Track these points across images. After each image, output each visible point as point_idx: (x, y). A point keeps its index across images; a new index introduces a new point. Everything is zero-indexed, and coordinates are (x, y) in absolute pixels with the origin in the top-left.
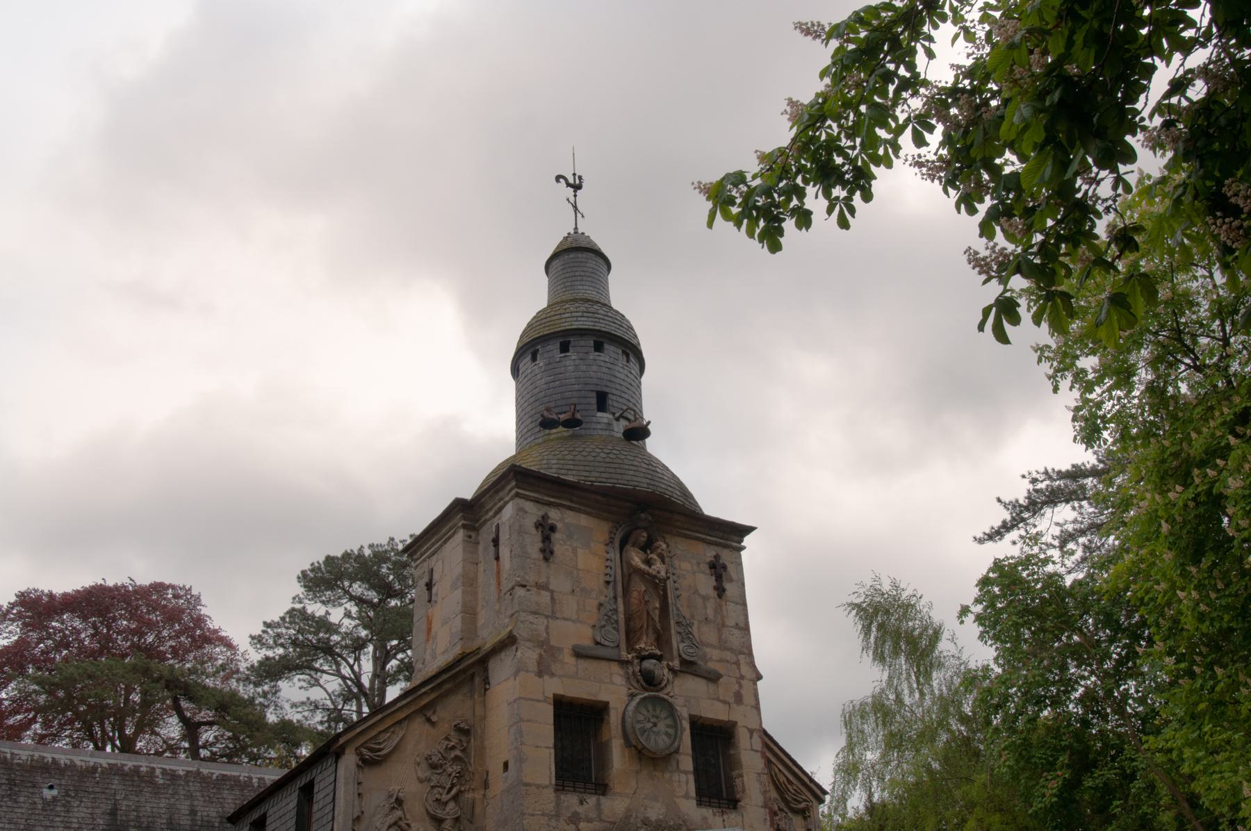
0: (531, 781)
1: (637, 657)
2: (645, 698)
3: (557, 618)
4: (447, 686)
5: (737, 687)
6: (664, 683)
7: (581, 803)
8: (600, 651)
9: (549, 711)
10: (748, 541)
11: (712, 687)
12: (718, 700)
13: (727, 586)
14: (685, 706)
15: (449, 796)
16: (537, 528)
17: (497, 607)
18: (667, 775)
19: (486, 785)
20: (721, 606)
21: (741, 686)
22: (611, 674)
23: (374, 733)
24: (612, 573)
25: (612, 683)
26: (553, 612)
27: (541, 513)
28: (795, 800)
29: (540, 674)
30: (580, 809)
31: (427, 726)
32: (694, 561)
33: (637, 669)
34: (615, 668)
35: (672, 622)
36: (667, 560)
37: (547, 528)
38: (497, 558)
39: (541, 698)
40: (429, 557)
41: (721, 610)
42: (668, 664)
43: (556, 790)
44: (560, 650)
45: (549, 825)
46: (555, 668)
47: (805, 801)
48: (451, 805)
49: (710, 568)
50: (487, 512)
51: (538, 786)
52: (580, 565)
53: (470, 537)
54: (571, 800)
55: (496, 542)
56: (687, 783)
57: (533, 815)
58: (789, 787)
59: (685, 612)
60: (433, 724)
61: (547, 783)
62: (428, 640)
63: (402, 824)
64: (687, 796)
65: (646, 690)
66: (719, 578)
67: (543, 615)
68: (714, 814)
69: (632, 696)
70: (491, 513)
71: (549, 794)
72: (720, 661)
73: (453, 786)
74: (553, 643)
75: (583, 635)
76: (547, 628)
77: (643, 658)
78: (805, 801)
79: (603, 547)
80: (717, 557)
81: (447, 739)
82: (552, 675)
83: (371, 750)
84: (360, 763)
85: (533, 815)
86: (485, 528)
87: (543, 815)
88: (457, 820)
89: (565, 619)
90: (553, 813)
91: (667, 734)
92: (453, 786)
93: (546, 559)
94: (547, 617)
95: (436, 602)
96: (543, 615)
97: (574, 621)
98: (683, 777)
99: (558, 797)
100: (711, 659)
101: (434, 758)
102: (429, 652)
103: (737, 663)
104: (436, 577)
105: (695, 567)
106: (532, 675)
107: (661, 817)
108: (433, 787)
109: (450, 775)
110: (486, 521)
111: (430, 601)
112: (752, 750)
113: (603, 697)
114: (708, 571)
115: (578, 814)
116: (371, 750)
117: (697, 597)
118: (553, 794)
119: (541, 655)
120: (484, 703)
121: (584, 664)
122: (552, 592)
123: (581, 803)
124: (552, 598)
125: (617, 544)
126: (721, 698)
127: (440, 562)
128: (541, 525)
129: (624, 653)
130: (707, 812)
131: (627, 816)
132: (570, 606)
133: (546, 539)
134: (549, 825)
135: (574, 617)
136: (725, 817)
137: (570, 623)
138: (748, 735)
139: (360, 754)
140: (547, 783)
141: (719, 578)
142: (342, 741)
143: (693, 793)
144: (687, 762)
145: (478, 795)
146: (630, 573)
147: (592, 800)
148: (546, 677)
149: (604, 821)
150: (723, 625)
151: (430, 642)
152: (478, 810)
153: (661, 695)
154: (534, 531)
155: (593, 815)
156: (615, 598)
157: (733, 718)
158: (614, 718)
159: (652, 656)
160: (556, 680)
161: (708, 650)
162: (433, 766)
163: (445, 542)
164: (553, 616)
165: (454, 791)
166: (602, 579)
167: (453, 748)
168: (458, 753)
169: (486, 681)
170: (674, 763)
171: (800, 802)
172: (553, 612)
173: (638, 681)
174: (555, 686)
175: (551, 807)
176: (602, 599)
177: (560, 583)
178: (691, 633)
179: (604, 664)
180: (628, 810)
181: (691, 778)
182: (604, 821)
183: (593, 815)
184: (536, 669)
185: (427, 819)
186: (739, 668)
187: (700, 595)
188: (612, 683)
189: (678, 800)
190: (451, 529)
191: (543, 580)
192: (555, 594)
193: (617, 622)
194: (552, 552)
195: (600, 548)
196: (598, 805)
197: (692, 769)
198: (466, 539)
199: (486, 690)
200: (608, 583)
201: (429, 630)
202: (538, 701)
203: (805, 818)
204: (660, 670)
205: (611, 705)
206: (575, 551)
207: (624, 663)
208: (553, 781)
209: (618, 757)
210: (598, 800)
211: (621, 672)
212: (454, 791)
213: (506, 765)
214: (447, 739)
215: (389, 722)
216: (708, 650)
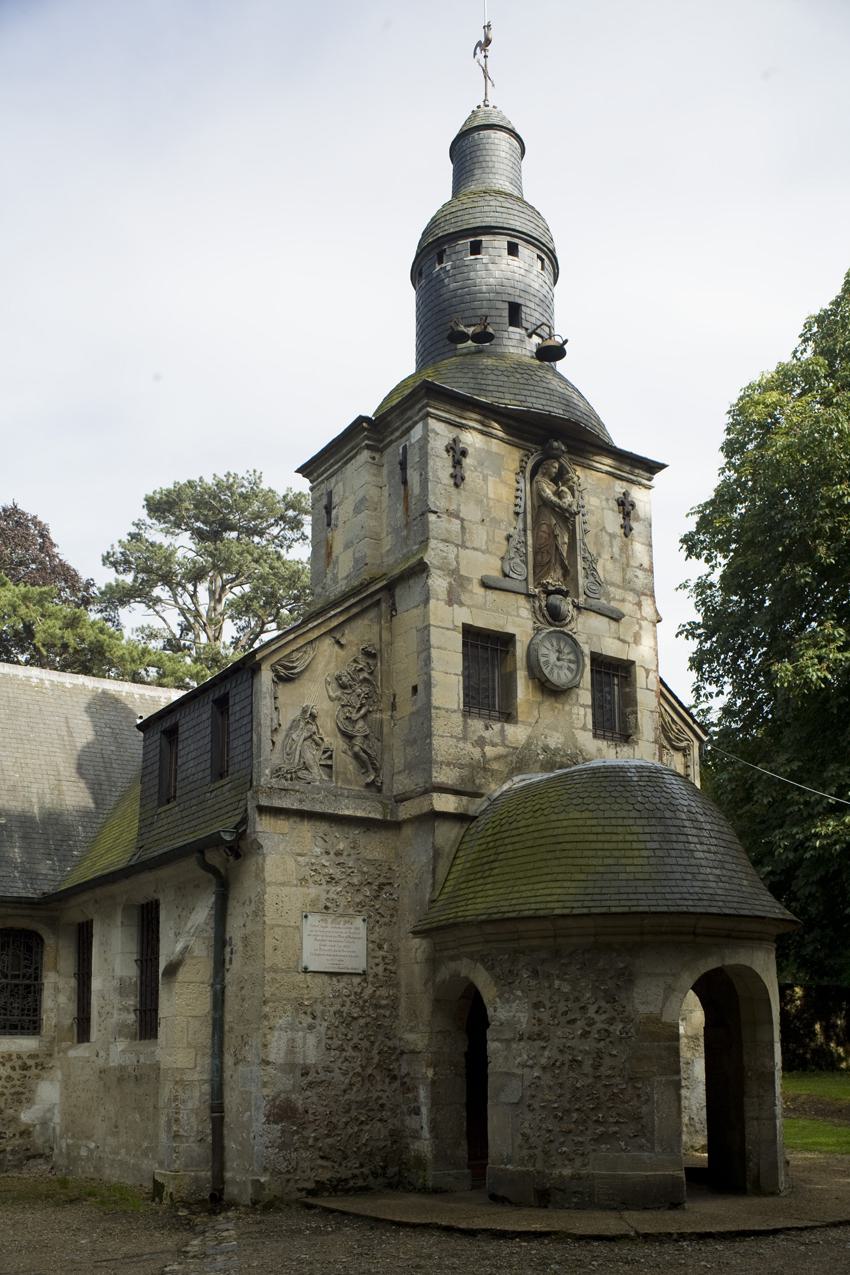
0: (441, 705)
1: (544, 592)
2: (550, 632)
3: (467, 548)
4: (355, 610)
6: (567, 621)
7: (487, 728)
8: (507, 583)
9: (457, 640)
10: (658, 477)
11: (613, 624)
13: (634, 525)
14: (587, 643)
15: (359, 715)
16: (448, 451)
17: (404, 533)
18: (567, 708)
19: (394, 707)
20: (626, 545)
22: (518, 608)
23: (287, 651)
24: (522, 504)
25: (518, 616)
26: (463, 542)
27: (452, 436)
28: (677, 738)
29: (450, 602)
30: (487, 734)
31: (336, 647)
32: (604, 497)
33: (544, 604)
34: (522, 601)
35: (579, 559)
36: (577, 493)
37: (459, 453)
38: (405, 482)
40: (327, 479)
41: (627, 550)
42: (573, 601)
43: (464, 716)
44: (469, 580)
45: (457, 747)
46: (464, 598)
47: (687, 740)
48: (361, 723)
49: (619, 505)
50: (392, 433)
51: (447, 711)
52: (491, 495)
53: (374, 458)
54: (477, 725)
55: (403, 465)
56: (585, 715)
57: (443, 737)
58: (674, 727)
59: (592, 548)
60: (341, 646)
61: (456, 707)
62: (328, 565)
63: (316, 737)
64: (584, 728)
65: (551, 625)
66: (626, 515)
67: (453, 543)
68: (609, 747)
69: (537, 630)
70: (397, 434)
71: (458, 718)
73: (362, 705)
74: (462, 573)
75: (492, 567)
76: (457, 556)
77: (549, 593)
78: (687, 740)
79: (513, 476)
81: (355, 661)
82: (461, 604)
83: (286, 668)
84: (276, 680)
85: (443, 737)
86: (390, 450)
87: (452, 736)
88: (366, 737)
89: (474, 549)
90: (461, 736)
91: (569, 669)
92: (362, 705)
93: (457, 485)
94: (457, 546)
95: (336, 526)
96: (453, 543)
97: (483, 552)
98: (582, 711)
99: (465, 722)
100: (614, 599)
101: (344, 678)
102: (329, 576)
104: (336, 499)
105: (604, 503)
106: (443, 603)
107: (560, 746)
108: (343, 706)
109: (359, 696)
110: (391, 442)
111: (329, 525)
113: (510, 629)
114: (616, 508)
115: (484, 738)
116: (286, 668)
117: (604, 533)
118: (461, 719)
119: (450, 583)
120: (390, 630)
121: (492, 595)
122: (462, 520)
123: (487, 728)
124: (463, 528)
125: (528, 475)
126: (622, 637)
127: (340, 484)
128: (451, 448)
129: (531, 587)
130: (602, 744)
131: (528, 744)
132: (479, 536)
133: (457, 464)
134: (457, 747)
135: (484, 547)
136: (618, 749)
137: (480, 553)
138: (645, 675)
139: (275, 671)
140: (456, 707)
141: (626, 515)
142: (258, 657)
143: (590, 726)
144: (585, 696)
145: (386, 716)
146: (542, 505)
147: (497, 726)
148: (455, 606)
149: (508, 747)
150: (628, 565)
151: (331, 566)
152: (386, 730)
153: (566, 630)
154: (445, 455)
155: (497, 740)
156: (525, 530)
158: (520, 650)
159: (559, 592)
160: (464, 609)
161: (612, 589)
162: (343, 687)
163: (346, 463)
164: (463, 546)
165: (363, 711)
166: (512, 508)
167: (361, 670)
168: (366, 675)
169: (393, 608)
170: (574, 697)
171: (682, 741)
172: (463, 542)
173: (544, 616)
174: (463, 616)
175: (458, 731)
176: (511, 531)
177: (470, 512)
178: (596, 570)
179: (511, 595)
180: (529, 737)
181: (589, 711)
182: (508, 747)
183: (497, 740)
184: (444, 595)
185: (339, 735)
187: (606, 532)
188: (518, 616)
189: (576, 732)
190: (353, 449)
191: (453, 507)
192: (465, 522)
193: (526, 554)
194: (463, 479)
195: (511, 477)
196: (502, 730)
197: (590, 703)
198: (370, 460)
199: (392, 616)
200: (517, 514)
201: (329, 555)
202: (448, 629)
203: (685, 756)
204: (566, 606)
205: (517, 637)
206: (485, 479)
207: (529, 596)
208: (462, 707)
209: (523, 690)
210: (503, 727)
211: (528, 606)
212: (363, 711)
213: (415, 689)
214: (355, 661)
215: (301, 642)
216: (612, 589)
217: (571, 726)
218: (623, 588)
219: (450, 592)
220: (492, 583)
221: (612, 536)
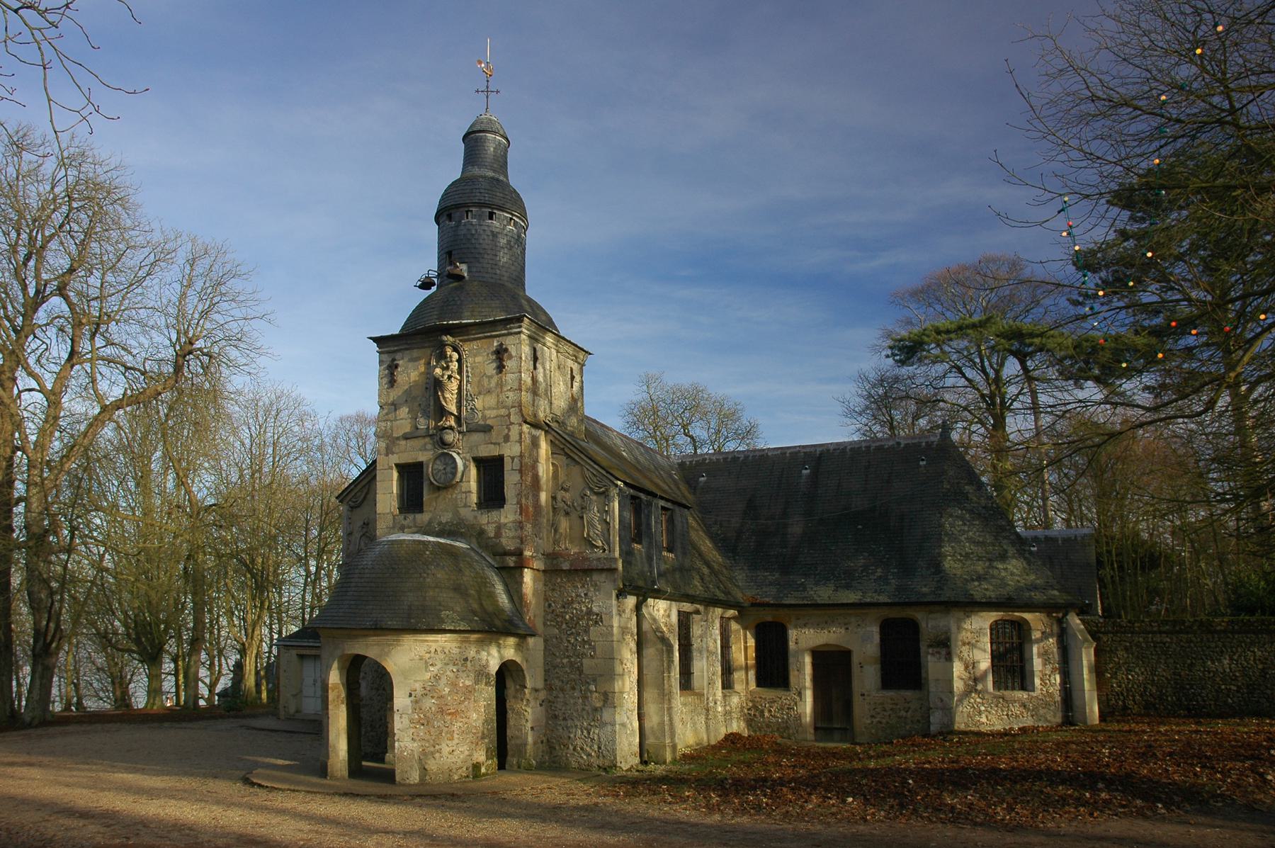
5: (506, 431)
11: (487, 436)
12: (492, 443)
21: (509, 430)
23: (353, 494)
39: (387, 467)
72: (497, 417)
80: (501, 345)
103: (509, 415)
112: (512, 470)
113: (420, 459)
119: (387, 445)
130: (478, 514)
131: (430, 522)
157: (501, 453)
174: (395, 459)
180: (430, 519)
184: (385, 452)
186: (509, 418)
196: (414, 518)
215: (359, 487)
217: (457, 506)
218: (498, 408)
219: (387, 448)
220: (408, 436)
221: (490, 377)
